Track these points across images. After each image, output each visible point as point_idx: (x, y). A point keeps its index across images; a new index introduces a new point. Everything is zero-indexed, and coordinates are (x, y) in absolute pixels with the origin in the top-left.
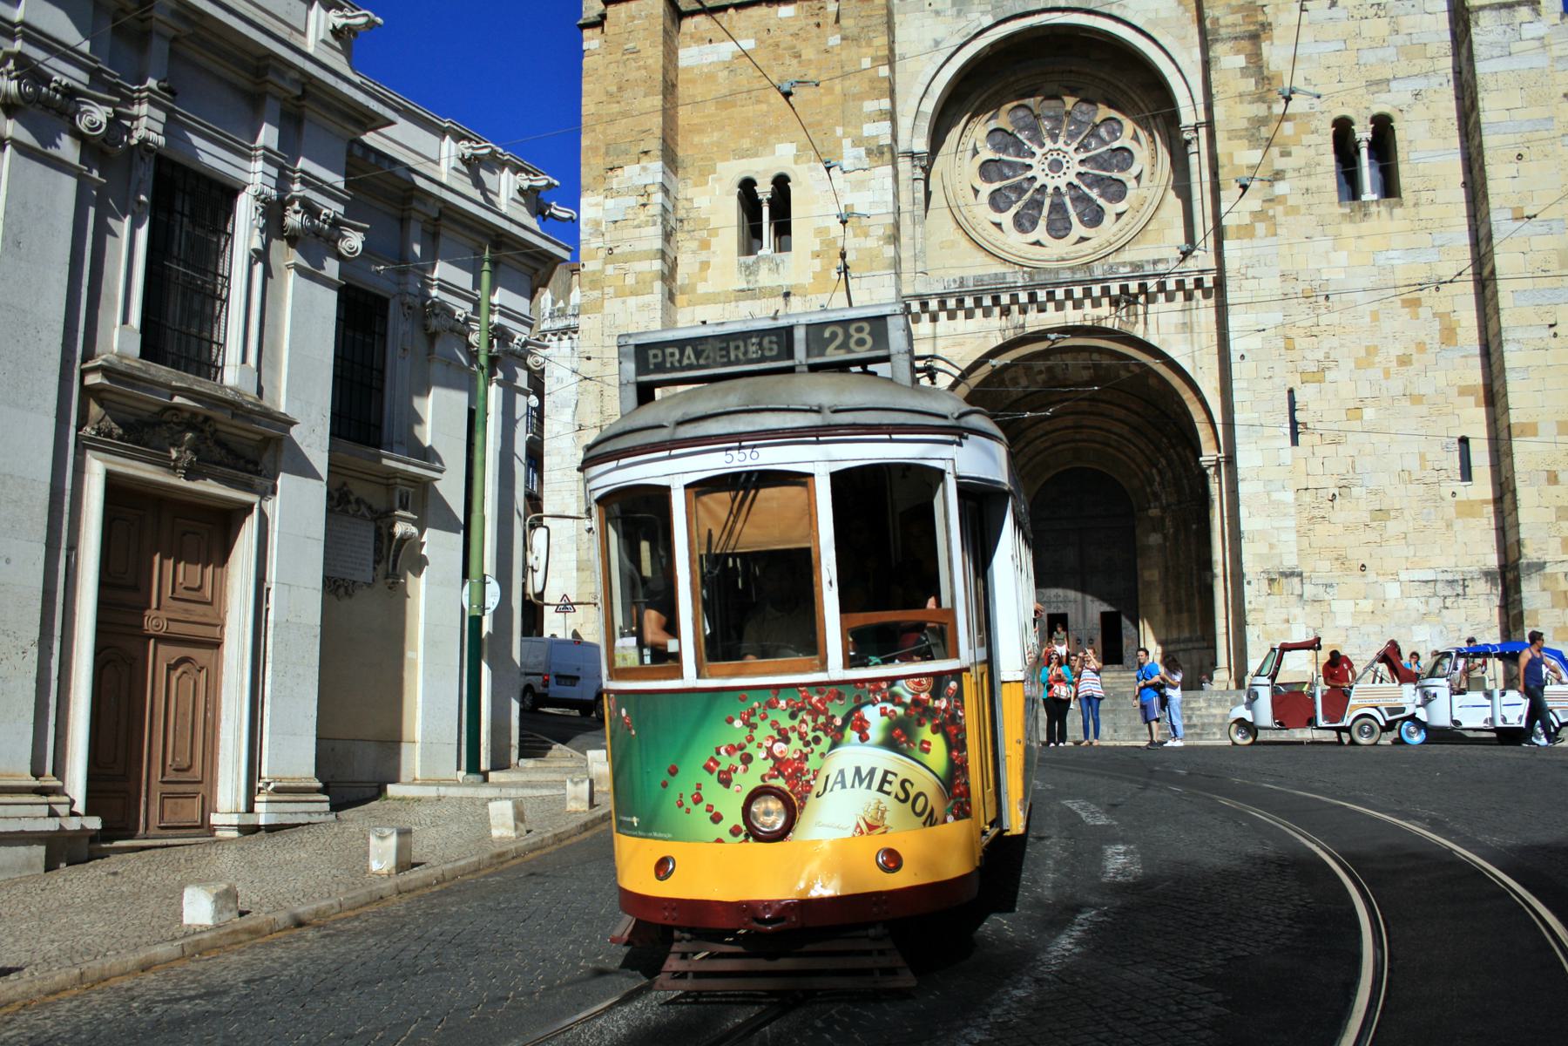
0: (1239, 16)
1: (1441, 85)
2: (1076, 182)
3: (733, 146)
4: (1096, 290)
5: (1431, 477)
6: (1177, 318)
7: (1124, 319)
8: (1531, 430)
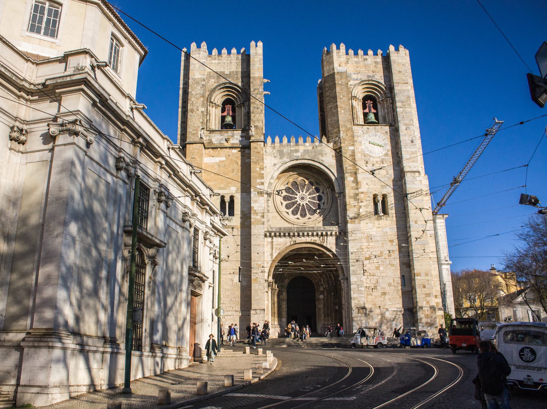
2: (308, 203)
3: (219, 186)
4: (315, 233)
5: (396, 285)
6: (334, 241)
8: (419, 275)
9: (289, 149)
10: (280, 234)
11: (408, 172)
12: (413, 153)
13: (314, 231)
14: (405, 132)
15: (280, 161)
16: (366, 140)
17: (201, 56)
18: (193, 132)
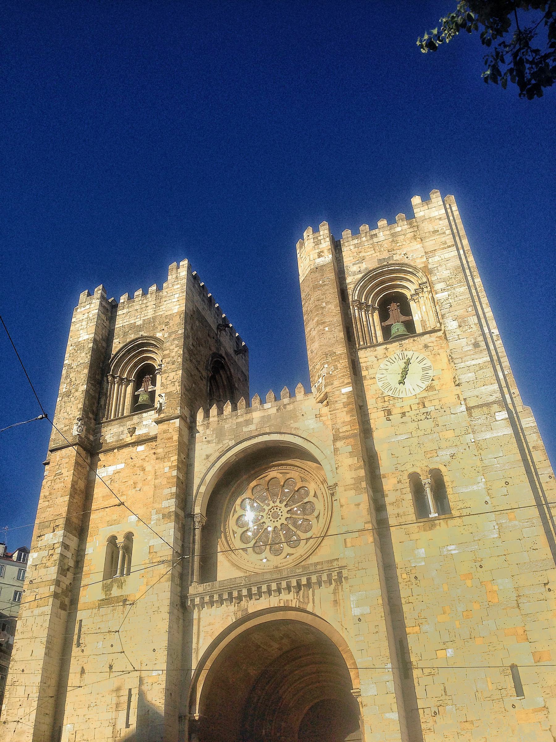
0: (349, 426)
1: (465, 449)
7: (302, 600)
9: (235, 423)
10: (212, 597)
11: (473, 407)
12: (481, 368)
13: (282, 579)
14: (458, 332)
15: (217, 448)
16: (384, 372)
17: (92, 305)
18: (65, 429)
